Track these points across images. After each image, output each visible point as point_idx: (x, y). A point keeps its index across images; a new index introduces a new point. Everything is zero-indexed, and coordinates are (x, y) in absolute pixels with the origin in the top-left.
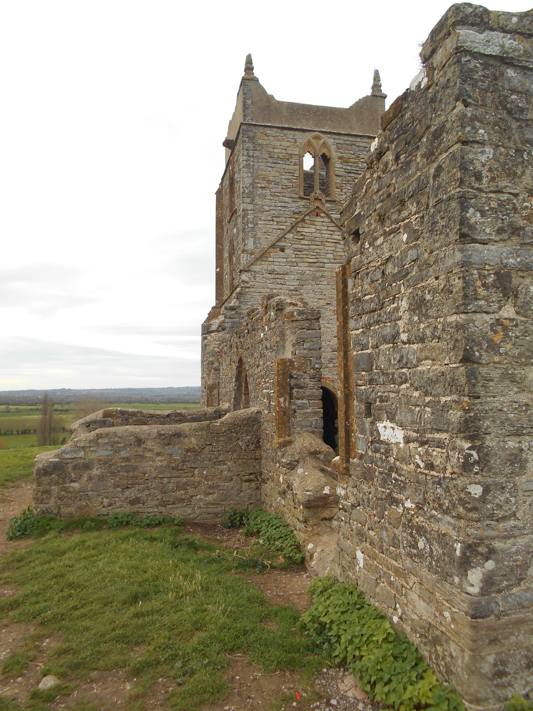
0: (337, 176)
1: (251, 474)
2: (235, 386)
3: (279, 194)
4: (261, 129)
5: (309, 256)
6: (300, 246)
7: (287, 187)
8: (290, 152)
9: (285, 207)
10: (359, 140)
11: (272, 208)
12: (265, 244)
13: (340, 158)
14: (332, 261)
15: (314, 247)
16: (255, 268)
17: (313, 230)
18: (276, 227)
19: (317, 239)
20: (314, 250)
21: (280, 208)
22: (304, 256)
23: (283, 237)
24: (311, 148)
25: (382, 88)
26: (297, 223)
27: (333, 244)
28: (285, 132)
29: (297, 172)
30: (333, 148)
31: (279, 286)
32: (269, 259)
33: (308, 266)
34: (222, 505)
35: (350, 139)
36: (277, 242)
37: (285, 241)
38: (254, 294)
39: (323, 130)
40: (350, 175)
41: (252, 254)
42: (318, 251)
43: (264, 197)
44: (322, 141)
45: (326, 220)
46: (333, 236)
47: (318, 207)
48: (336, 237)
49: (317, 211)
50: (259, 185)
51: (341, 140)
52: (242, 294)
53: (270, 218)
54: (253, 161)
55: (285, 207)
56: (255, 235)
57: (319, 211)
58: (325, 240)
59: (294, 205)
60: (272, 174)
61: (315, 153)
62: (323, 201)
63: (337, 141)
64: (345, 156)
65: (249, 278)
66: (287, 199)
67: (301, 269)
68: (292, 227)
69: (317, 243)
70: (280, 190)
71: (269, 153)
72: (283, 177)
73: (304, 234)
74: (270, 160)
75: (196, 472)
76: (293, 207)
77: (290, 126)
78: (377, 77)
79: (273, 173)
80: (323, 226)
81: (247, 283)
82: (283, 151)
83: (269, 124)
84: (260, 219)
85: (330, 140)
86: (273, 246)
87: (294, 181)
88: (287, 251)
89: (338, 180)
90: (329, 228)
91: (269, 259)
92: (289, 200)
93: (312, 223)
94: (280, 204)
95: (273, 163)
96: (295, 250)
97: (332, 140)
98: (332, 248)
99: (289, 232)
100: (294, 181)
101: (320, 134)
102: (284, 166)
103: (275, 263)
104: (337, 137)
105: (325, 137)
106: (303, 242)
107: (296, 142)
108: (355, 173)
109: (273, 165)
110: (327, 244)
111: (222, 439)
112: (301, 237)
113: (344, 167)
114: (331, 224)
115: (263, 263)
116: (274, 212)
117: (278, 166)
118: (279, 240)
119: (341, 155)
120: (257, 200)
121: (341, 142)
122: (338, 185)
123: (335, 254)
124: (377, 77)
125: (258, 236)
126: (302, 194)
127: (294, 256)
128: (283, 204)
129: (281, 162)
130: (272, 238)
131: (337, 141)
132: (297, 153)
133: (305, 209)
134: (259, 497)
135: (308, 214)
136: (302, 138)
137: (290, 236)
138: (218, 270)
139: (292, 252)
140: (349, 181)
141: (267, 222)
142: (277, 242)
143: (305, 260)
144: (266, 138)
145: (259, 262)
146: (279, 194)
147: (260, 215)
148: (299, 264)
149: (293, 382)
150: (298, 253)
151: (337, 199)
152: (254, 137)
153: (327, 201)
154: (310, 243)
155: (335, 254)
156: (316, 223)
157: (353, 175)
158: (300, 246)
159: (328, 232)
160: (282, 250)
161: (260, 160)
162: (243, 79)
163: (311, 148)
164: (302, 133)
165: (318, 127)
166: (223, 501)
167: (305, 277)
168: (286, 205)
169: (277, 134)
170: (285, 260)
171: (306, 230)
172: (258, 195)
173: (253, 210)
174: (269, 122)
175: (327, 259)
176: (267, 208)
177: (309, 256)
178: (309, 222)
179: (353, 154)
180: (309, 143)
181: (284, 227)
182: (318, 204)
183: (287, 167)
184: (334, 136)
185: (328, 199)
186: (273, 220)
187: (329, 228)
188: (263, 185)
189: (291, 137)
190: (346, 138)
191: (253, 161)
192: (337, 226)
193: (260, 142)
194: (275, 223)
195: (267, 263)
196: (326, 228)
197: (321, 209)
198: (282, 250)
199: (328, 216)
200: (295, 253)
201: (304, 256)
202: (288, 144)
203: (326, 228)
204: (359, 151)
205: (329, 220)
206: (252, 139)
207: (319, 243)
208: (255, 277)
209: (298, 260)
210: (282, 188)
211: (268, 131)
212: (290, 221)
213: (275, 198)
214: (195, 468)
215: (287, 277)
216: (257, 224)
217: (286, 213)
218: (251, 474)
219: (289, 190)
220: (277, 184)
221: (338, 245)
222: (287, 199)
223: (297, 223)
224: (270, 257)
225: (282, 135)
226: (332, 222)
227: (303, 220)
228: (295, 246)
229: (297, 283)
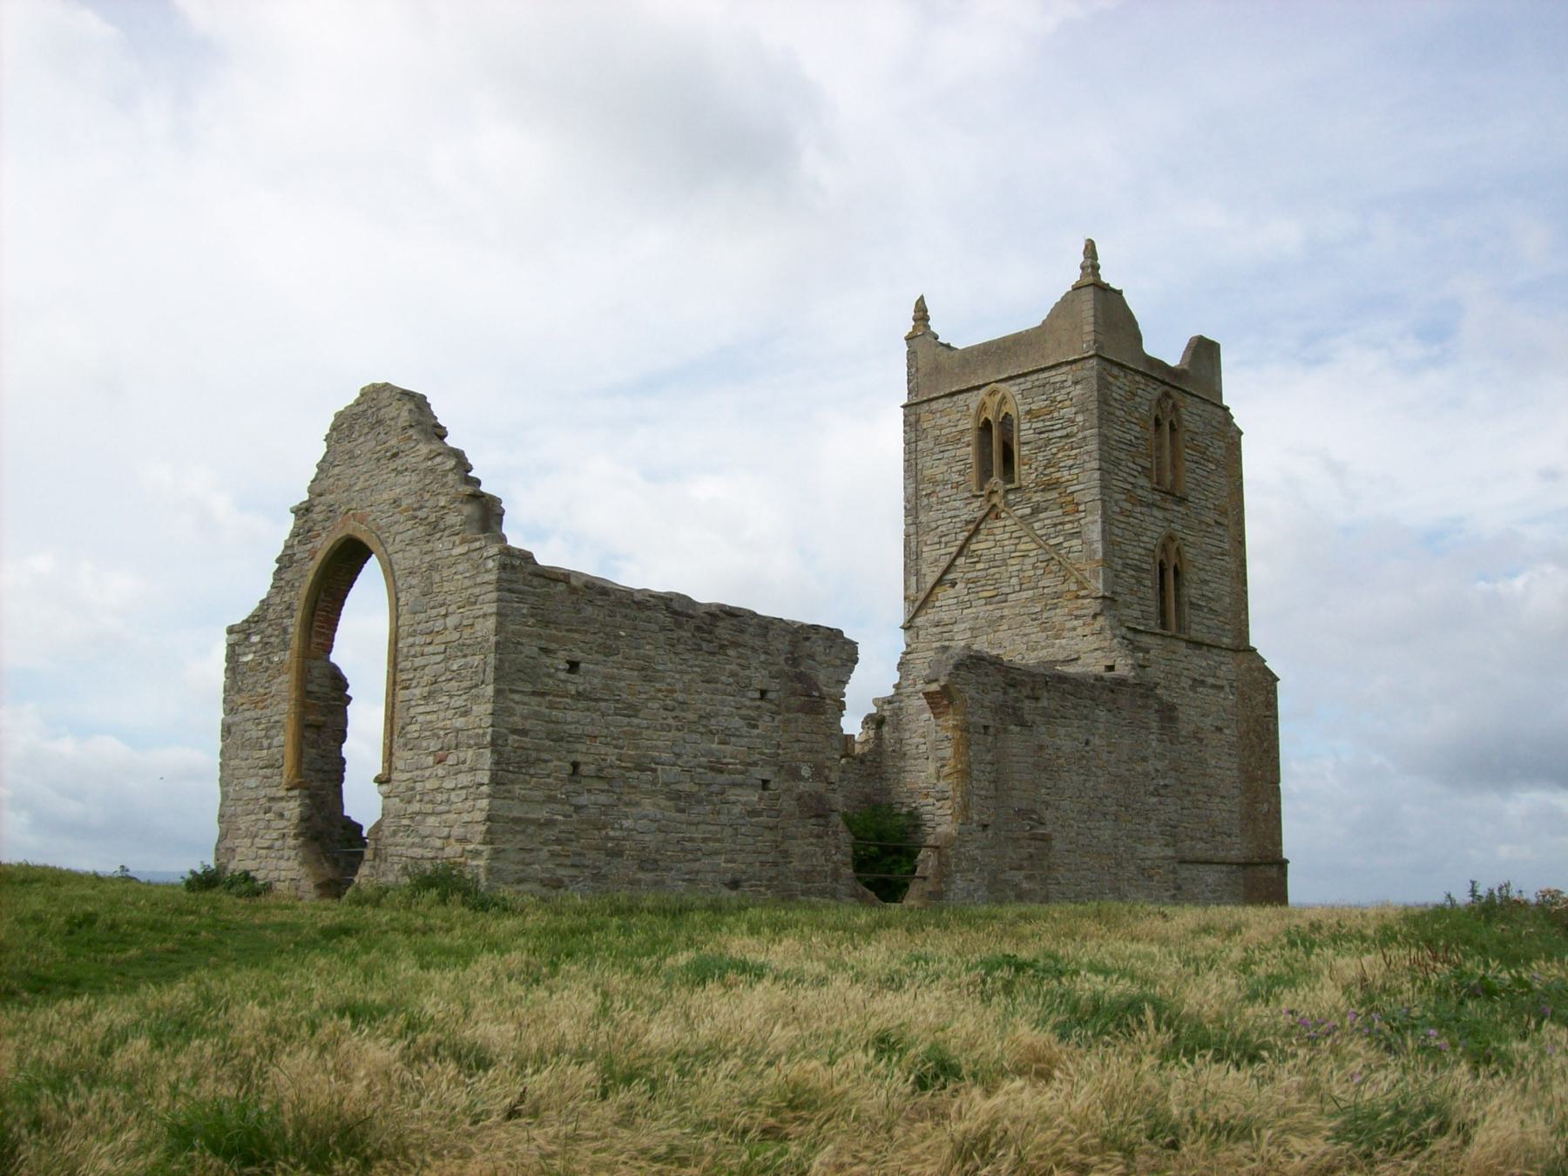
4: (926, 407)
7: (958, 484)
8: (960, 428)
12: (930, 580)
13: (1029, 412)
16: (919, 621)
47: (994, 506)
48: (1022, 547)
64: (1034, 407)
66: (957, 504)
68: (962, 548)
70: (949, 492)
71: (936, 438)
74: (937, 449)
78: (1090, 250)
85: (1011, 389)
86: (939, 582)
89: (1025, 450)
96: (969, 581)
99: (959, 554)
101: (999, 385)
106: (979, 566)
117: (946, 454)
118: (946, 571)
120: (923, 518)
121: (1029, 385)
124: (1090, 250)
137: (961, 561)
152: (918, 421)
153: (1007, 491)
160: (954, 584)
171: (982, 546)
176: (933, 525)
190: (1035, 377)
211: (934, 405)
212: (962, 536)
222: (957, 504)
223: (968, 539)
228: (969, 575)
229: (968, 634)
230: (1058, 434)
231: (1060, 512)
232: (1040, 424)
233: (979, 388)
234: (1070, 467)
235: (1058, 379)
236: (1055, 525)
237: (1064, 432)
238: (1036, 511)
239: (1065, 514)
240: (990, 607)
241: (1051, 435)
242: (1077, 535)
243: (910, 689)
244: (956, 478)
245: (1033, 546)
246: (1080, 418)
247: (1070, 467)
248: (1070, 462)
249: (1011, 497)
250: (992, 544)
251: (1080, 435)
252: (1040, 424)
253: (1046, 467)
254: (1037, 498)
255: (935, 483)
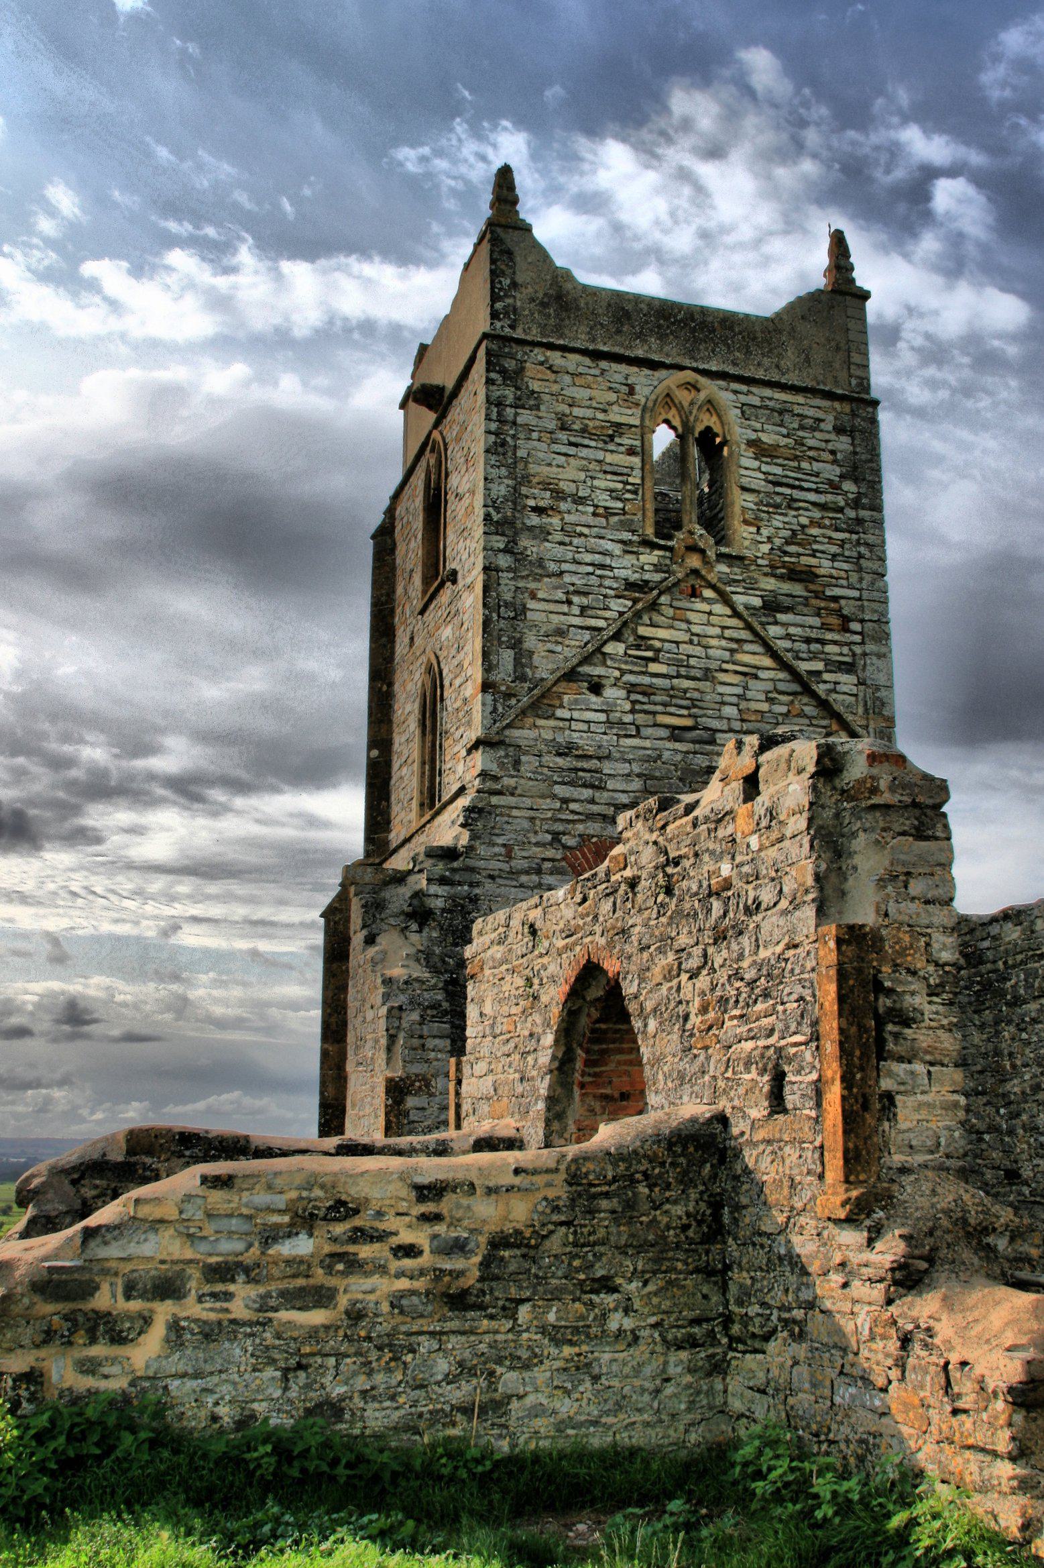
0: (744, 489)
1: (696, 1322)
2: (554, 1058)
3: (586, 531)
4: (539, 354)
5: (672, 710)
6: (646, 680)
7: (608, 513)
9: (602, 566)
10: (800, 399)
11: (565, 567)
12: (545, 666)
13: (751, 443)
14: (737, 725)
15: (686, 684)
17: (682, 636)
18: (577, 621)
19: (692, 662)
20: (685, 691)
21: (590, 569)
22: (659, 708)
23: (599, 650)
24: (674, 411)
25: (854, 274)
26: (638, 615)
27: (736, 679)
28: (604, 364)
29: (637, 472)
30: (734, 414)
31: (587, 793)
32: (560, 713)
33: (669, 739)
34: (608, 1427)
35: (777, 395)
36: (580, 664)
37: (604, 664)
38: (515, 813)
39: (701, 367)
40: (779, 489)
41: (508, 695)
42: (696, 695)
43: (543, 534)
44: (702, 396)
45: (719, 608)
46: (739, 657)
47: (695, 572)
49: (693, 581)
50: (531, 503)
51: (756, 396)
52: (480, 811)
53: (560, 595)
54: (513, 436)
55: (602, 566)
56: (520, 641)
57: (698, 582)
58: (714, 665)
59: (629, 560)
60: (568, 475)
61: (685, 424)
62: (711, 554)
63: (743, 398)
64: (765, 438)
65: (502, 765)
66: (609, 546)
67: (647, 743)
69: (693, 673)
70: (590, 520)
72: (596, 483)
73: (657, 644)
74: (563, 436)
75: (524, 1312)
76: (626, 568)
77: (617, 350)
79: (571, 472)
80: (709, 624)
81: (496, 778)
82: (600, 416)
83: (561, 342)
84: (533, 596)
85: (725, 396)
86: (571, 676)
87: (628, 496)
88: (610, 693)
90: (727, 633)
91: (560, 713)
92: (617, 549)
93: (680, 617)
94: (588, 558)
95: (571, 444)
96: (631, 688)
97: (732, 396)
98: (739, 691)
100: (628, 496)
102: (600, 455)
103: (574, 725)
104: (744, 388)
105: (710, 388)
106: (654, 667)
107: (632, 391)
108: (793, 487)
109: (572, 450)
110: (722, 677)
111: (604, 1204)
112: (650, 654)
113: (764, 468)
114: (734, 622)
115: (540, 722)
116: (575, 579)
117: (584, 452)
119: (753, 436)
121: (756, 401)
122: (749, 516)
123: (743, 705)
125: (526, 646)
126: (650, 531)
127: (628, 707)
128: (598, 558)
129: (593, 444)
130: (569, 651)
131: (743, 398)
132: (637, 423)
133: (657, 577)
134: (719, 1400)
135: (668, 590)
136: (645, 383)
138: (375, 753)
139: (622, 693)
140: (777, 506)
141: (552, 607)
142: (580, 664)
143: (661, 719)
144: (552, 377)
145: (529, 721)
146: (586, 531)
147: (532, 585)
148: (646, 732)
149: (884, 1002)
150: (640, 697)
151: (747, 553)
153: (721, 557)
154: (672, 671)
155: (743, 705)
156: (691, 616)
157: (788, 491)
158: (646, 680)
159: (724, 643)
160: (596, 688)
161: (535, 435)
162: (491, 224)
163: (674, 411)
164: (646, 372)
165: (693, 358)
166: (607, 1413)
167: (659, 770)
168: (608, 561)
169: (581, 369)
170: (602, 717)
172: (531, 529)
173: (514, 571)
174: (561, 336)
175: (720, 718)
176: (552, 567)
177: (672, 710)
178: (670, 612)
179: (787, 436)
180: (669, 400)
181: (601, 623)
182: (694, 561)
183: (609, 458)
184: (735, 386)
185: (724, 550)
186: (569, 603)
187: (727, 633)
188: (542, 504)
189: (619, 378)
190: (767, 392)
191: (513, 436)
192: (749, 627)
193: (535, 386)
194: (576, 611)
195: (552, 723)
196: (718, 631)
197: (703, 578)
198: (596, 688)
199: (725, 599)
200: (634, 697)
201: (659, 708)
202: (613, 397)
203: (718, 631)
204: (802, 427)
205: (728, 612)
206: (514, 377)
207: (699, 674)
208: (517, 763)
209: (641, 718)
210: (594, 514)
211: (556, 358)
213: (576, 541)
214: (523, 1301)
215: (608, 767)
216: (525, 609)
217: (607, 583)
218: (696, 1322)
219: (616, 518)
220: (579, 500)
221: (752, 683)
222: (609, 546)
224: (562, 706)
225: (593, 372)
226: (736, 614)
227: (654, 606)
229: (637, 784)
230: (812, 497)
231: (816, 621)
232: (778, 470)
233: (654, 365)
234: (834, 557)
235: (811, 412)
236: (808, 641)
237: (821, 499)
238: (772, 606)
239: (825, 627)
240: (678, 746)
241: (797, 494)
242: (849, 668)
243: (495, 865)
244: (603, 499)
245: (767, 662)
246: (849, 486)
247: (834, 557)
248: (834, 549)
249: (723, 568)
250: (686, 637)
251: (852, 514)
252: (778, 470)
253: (787, 543)
254: (770, 584)
255: (559, 495)
